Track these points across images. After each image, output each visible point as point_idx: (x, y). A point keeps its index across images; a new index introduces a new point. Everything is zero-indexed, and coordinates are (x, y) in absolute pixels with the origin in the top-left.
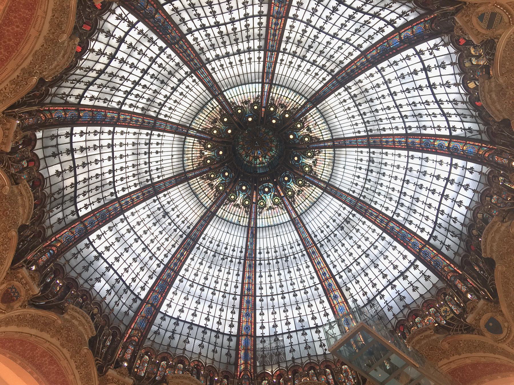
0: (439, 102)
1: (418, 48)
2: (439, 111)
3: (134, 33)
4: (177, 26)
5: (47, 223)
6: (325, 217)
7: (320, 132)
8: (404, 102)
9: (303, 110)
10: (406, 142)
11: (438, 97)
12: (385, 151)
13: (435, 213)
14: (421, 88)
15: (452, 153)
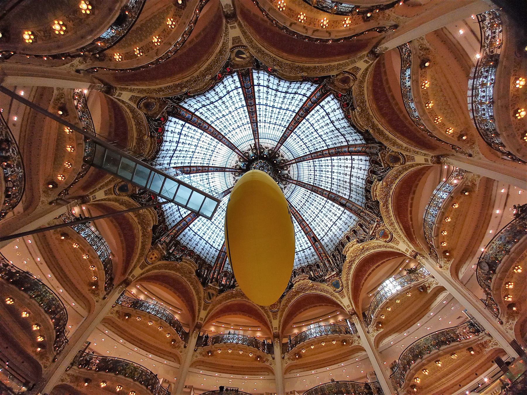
0: (338, 129)
1: (321, 104)
2: (339, 134)
3: (185, 129)
4: (205, 122)
5: (168, 223)
6: (299, 197)
7: (288, 156)
8: (322, 133)
9: (278, 148)
10: (329, 153)
11: (337, 127)
12: (320, 159)
13: (349, 185)
14: (328, 124)
15: (351, 153)
